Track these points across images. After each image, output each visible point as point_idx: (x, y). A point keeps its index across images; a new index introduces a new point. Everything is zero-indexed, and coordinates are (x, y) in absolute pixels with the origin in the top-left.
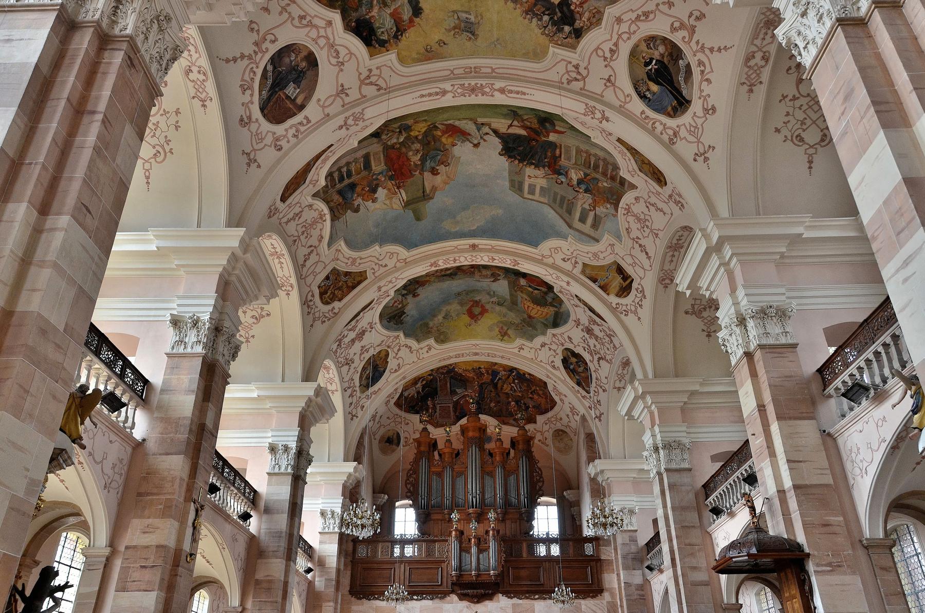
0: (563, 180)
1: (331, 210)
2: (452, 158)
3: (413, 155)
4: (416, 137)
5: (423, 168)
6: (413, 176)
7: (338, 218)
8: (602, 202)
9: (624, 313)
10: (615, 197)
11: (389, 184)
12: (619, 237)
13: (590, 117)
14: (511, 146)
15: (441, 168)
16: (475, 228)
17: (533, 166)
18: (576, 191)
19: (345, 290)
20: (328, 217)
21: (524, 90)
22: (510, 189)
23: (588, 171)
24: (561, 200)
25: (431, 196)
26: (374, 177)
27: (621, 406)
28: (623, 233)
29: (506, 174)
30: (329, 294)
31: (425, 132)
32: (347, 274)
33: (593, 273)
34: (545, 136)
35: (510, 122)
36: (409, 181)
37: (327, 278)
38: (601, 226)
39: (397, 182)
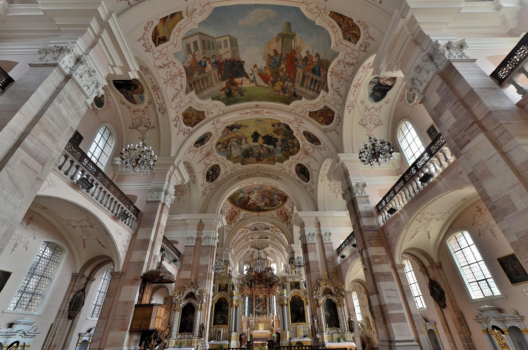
0: (213, 60)
1: (327, 70)
2: (266, 59)
3: (284, 69)
4: (281, 80)
5: (281, 57)
7: (327, 60)
8: (192, 64)
9: (147, 26)
10: (189, 73)
11: (298, 57)
12: (176, 55)
14: (240, 69)
15: (272, 54)
17: (228, 60)
18: (205, 58)
19: (346, 20)
20: (330, 70)
23: (205, 75)
24: (210, 46)
26: (303, 67)
27: (183, 167)
29: (240, 49)
30: (354, 32)
31: (276, 82)
32: (340, 26)
33: (175, 18)
35: (243, 86)
37: (349, 40)
39: (294, 55)
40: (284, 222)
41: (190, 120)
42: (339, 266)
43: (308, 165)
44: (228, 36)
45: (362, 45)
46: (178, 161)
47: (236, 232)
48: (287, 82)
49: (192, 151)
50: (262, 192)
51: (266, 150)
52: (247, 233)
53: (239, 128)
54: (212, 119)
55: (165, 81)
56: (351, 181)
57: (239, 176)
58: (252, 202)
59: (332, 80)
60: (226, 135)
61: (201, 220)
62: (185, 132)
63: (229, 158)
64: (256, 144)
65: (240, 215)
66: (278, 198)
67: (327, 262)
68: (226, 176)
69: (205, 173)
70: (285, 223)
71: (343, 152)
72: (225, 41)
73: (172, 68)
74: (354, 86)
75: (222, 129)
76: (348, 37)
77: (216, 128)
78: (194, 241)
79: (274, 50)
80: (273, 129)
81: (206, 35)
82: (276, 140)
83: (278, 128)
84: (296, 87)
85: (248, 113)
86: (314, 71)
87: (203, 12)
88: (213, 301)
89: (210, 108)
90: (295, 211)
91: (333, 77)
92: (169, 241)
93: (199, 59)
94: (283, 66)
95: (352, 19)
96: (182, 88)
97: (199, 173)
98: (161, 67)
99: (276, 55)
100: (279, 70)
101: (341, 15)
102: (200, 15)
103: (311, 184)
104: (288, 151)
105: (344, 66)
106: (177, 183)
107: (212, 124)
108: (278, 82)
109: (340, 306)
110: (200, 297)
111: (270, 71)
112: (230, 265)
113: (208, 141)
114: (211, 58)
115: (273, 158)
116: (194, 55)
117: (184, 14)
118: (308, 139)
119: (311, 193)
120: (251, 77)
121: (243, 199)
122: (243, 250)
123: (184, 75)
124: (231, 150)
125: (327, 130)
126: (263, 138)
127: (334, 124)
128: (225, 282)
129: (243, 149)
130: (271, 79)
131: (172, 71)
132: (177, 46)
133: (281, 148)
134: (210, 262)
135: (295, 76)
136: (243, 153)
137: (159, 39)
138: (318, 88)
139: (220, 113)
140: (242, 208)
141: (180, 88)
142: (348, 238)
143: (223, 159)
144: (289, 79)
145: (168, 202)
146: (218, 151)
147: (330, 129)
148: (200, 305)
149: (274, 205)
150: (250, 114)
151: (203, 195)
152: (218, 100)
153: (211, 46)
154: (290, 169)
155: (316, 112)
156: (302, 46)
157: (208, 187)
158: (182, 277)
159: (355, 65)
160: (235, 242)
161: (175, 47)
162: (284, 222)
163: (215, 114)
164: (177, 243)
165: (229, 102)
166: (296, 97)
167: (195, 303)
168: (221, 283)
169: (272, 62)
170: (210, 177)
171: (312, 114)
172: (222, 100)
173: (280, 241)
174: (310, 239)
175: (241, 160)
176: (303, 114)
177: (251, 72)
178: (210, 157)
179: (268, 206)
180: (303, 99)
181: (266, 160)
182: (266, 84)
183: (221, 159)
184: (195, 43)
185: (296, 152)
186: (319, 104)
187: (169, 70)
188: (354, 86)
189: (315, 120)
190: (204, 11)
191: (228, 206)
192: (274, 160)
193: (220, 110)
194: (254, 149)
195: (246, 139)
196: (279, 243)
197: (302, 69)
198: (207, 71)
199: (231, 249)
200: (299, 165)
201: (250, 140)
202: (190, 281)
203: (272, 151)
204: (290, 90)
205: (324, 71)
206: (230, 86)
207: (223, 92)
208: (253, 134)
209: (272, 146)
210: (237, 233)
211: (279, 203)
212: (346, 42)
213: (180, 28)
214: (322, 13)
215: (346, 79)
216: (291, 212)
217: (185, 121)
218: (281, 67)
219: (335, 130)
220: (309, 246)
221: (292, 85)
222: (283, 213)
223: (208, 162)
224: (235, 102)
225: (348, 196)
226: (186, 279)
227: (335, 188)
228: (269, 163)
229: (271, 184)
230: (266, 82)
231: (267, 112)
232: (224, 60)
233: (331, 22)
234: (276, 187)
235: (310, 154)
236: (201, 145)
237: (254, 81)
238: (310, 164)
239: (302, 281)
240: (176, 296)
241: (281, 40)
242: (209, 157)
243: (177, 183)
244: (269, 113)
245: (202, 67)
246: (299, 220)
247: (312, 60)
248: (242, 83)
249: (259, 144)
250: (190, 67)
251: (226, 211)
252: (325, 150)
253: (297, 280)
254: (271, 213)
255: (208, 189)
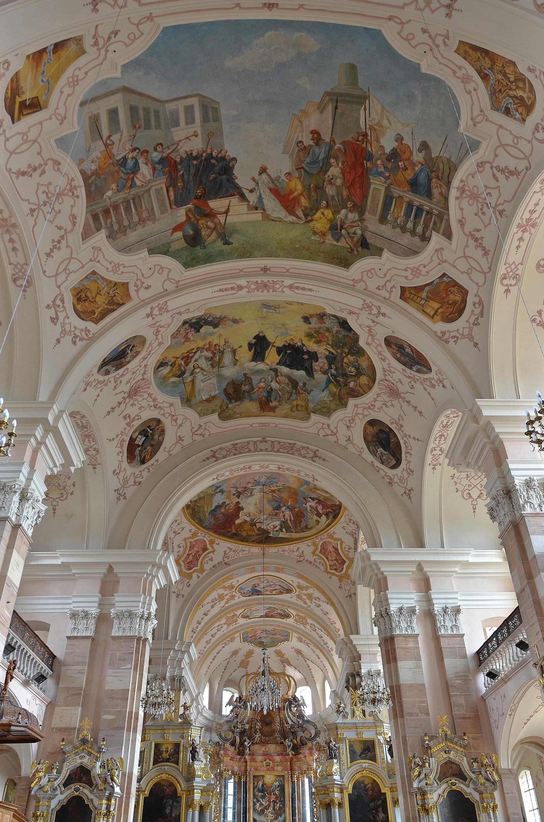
0: (155, 154)
1: (448, 184)
2: (292, 154)
4: (327, 206)
6: (344, 143)
7: (449, 160)
8: (102, 164)
10: (93, 188)
11: (373, 149)
13: (161, 303)
14: (224, 177)
15: (308, 141)
16: (269, 33)
17: (194, 154)
18: (134, 150)
19: (498, 66)
20: (456, 183)
21: (221, 293)
22: (219, 103)
23: (133, 191)
24: (149, 121)
25: (327, 98)
26: (387, 174)
28: (59, 155)
29: (226, 128)
30: (520, 93)
31: (317, 210)
32: (485, 77)
33: (64, 54)
34: (190, 210)
35: (230, 219)
36: (349, 138)
37: (507, 112)
38: (88, 130)
39: (364, 145)
40: (333, 574)
41: (92, 304)
42: (483, 699)
43: (396, 423)
44: (195, 95)
45: (540, 127)
46: (56, 412)
47: (204, 599)
48: (343, 211)
49: (94, 384)
50: (273, 491)
51: (287, 381)
52: (232, 602)
53: (216, 326)
54: (148, 303)
55: (33, 207)
56: (513, 473)
57: (214, 449)
58: (248, 519)
59: (462, 209)
60: (183, 343)
61: (110, 568)
62: (76, 336)
63: (187, 401)
64: (260, 366)
65: (213, 551)
66: (316, 509)
67: (450, 690)
68: (178, 448)
69: (123, 440)
70: (335, 579)
71: (490, 396)
72: (189, 110)
73: (51, 175)
74: (519, 226)
75: (171, 326)
76: (503, 104)
77: (157, 324)
78: (92, 624)
79: (313, 132)
80: (305, 327)
81: (141, 94)
82: (314, 356)
83: (318, 326)
84: (367, 223)
85: (240, 288)
86: (414, 185)
87: (135, 38)
88: (138, 790)
89: (143, 275)
90: (363, 546)
91: (464, 203)
92: (25, 624)
93: (119, 153)
94: (334, 171)
95: (514, 64)
96: (74, 224)
97: (110, 440)
98: (24, 174)
99: (317, 144)
100: (324, 181)
101: (486, 53)
102: (127, 46)
103: (405, 473)
104: (346, 384)
105: (494, 175)
106: (52, 470)
107: (148, 316)
108: (321, 210)
109: (485, 809)
110: (105, 781)
111: (302, 183)
112: (185, 691)
113: (134, 357)
114: (151, 149)
115: (304, 404)
116: (108, 142)
117: (88, 43)
118: (398, 355)
119: (405, 498)
120: (252, 198)
121: (223, 510)
122: (220, 647)
123: (82, 192)
124: (193, 381)
125: (447, 335)
126: (279, 351)
127: (467, 321)
128: (172, 737)
129: (225, 379)
130: (304, 201)
131: (50, 183)
132: (66, 121)
133: (324, 378)
134: (134, 683)
135: (365, 196)
136: (225, 390)
137: (23, 105)
138: (426, 227)
139: (170, 286)
140: (220, 534)
141: (68, 225)
142: (506, 622)
143: (172, 405)
144: (349, 204)
145: (29, 522)
146: (161, 384)
147: (456, 334)
148: (104, 802)
149: (307, 528)
150: (245, 290)
151: (118, 499)
152: (166, 253)
153: (153, 121)
154: (349, 433)
155: (419, 289)
156: (385, 123)
157: (133, 478)
158: (56, 723)
159: (522, 174)
160: (200, 627)
161: (61, 124)
162: (333, 574)
163: (156, 289)
164: (46, 627)
165: (193, 259)
166: (368, 248)
167: (91, 796)
168: (160, 740)
169: (308, 160)
170: (137, 452)
171: (407, 294)
172: (174, 255)
173: (321, 625)
174: (403, 625)
175: (221, 407)
176: (384, 293)
177: (252, 185)
178: (140, 399)
179: (288, 530)
180: (386, 254)
181: (285, 408)
182: (290, 214)
183: (168, 405)
184: (113, 113)
185: (367, 390)
186: (428, 268)
187: (44, 180)
188: (519, 226)
189: (417, 309)
190: (138, 34)
191: (183, 528)
192: (307, 409)
193: (168, 279)
194: (255, 379)
195: (234, 352)
196: (318, 631)
197: (383, 180)
198: (138, 183)
199: (189, 645)
200: (372, 423)
201: (245, 355)
202: (78, 737)
203: (301, 384)
204: (352, 230)
205: (440, 185)
206: (198, 220)
207: (179, 234)
208: (254, 341)
209: (302, 373)
210: (206, 602)
211: (318, 522)
212: (499, 118)
213: (77, 76)
214: (438, 46)
215: (500, 208)
216: (352, 546)
217: (79, 307)
218: (329, 173)
219: (470, 337)
220: (399, 644)
221: (357, 218)
222: (330, 548)
223: (133, 411)
224: (208, 259)
225: (502, 513)
226: (69, 730)
227: (469, 486)
228: (293, 414)
229: (299, 471)
230: (291, 211)
231: (291, 287)
232: (184, 156)
233: (460, 68)
234: (310, 480)
235: (402, 395)
236: (117, 368)
237: (258, 207)
238: (401, 422)
239: (381, 738)
240: (40, 778)
241: (330, 108)
242: (137, 400)
243: (52, 470)
244: (297, 288)
245: (127, 173)
246: (373, 571)
247: (409, 159)
248: (227, 212)
249: (268, 367)
250: (96, 173)
251: (178, 540)
252: (444, 386)
253: (367, 735)
254: (298, 549)
255: (131, 482)
